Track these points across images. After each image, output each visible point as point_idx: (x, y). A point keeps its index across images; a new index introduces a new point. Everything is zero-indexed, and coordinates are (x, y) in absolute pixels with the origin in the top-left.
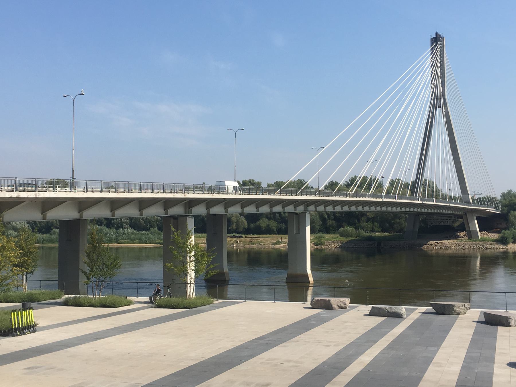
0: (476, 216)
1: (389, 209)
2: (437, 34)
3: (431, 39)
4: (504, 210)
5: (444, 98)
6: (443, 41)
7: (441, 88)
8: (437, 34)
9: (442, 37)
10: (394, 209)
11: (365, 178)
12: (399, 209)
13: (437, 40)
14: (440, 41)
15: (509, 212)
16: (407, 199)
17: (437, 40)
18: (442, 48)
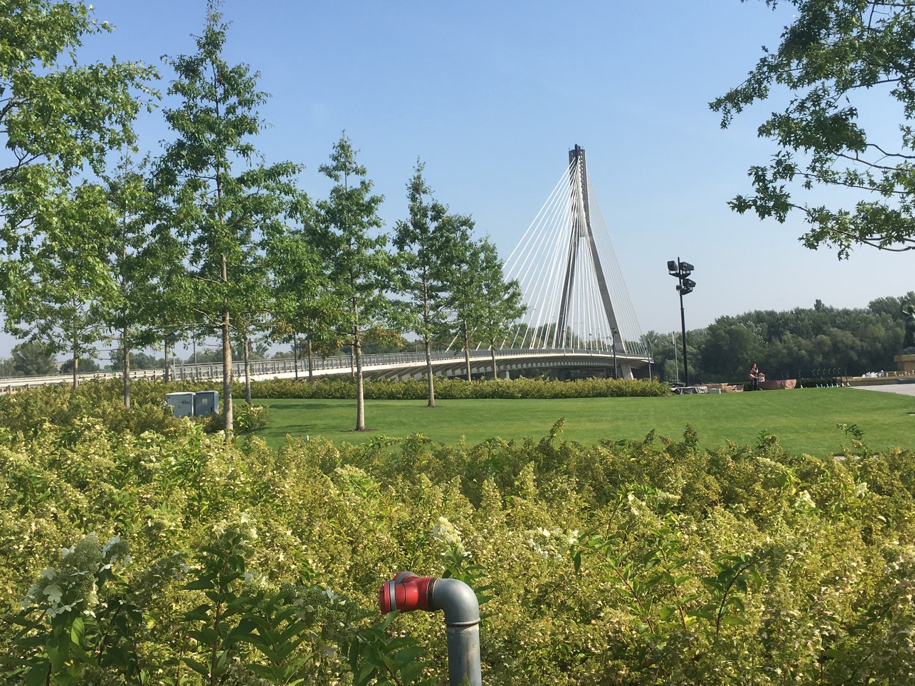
0: (632, 369)
1: (519, 366)
2: (576, 146)
3: (570, 152)
4: (657, 359)
5: (588, 225)
6: (584, 155)
7: (584, 213)
8: (576, 146)
9: (582, 150)
10: (525, 366)
11: (540, 328)
12: (530, 365)
13: (576, 154)
14: (580, 155)
15: (664, 361)
16: (544, 352)
17: (576, 154)
18: (583, 163)
